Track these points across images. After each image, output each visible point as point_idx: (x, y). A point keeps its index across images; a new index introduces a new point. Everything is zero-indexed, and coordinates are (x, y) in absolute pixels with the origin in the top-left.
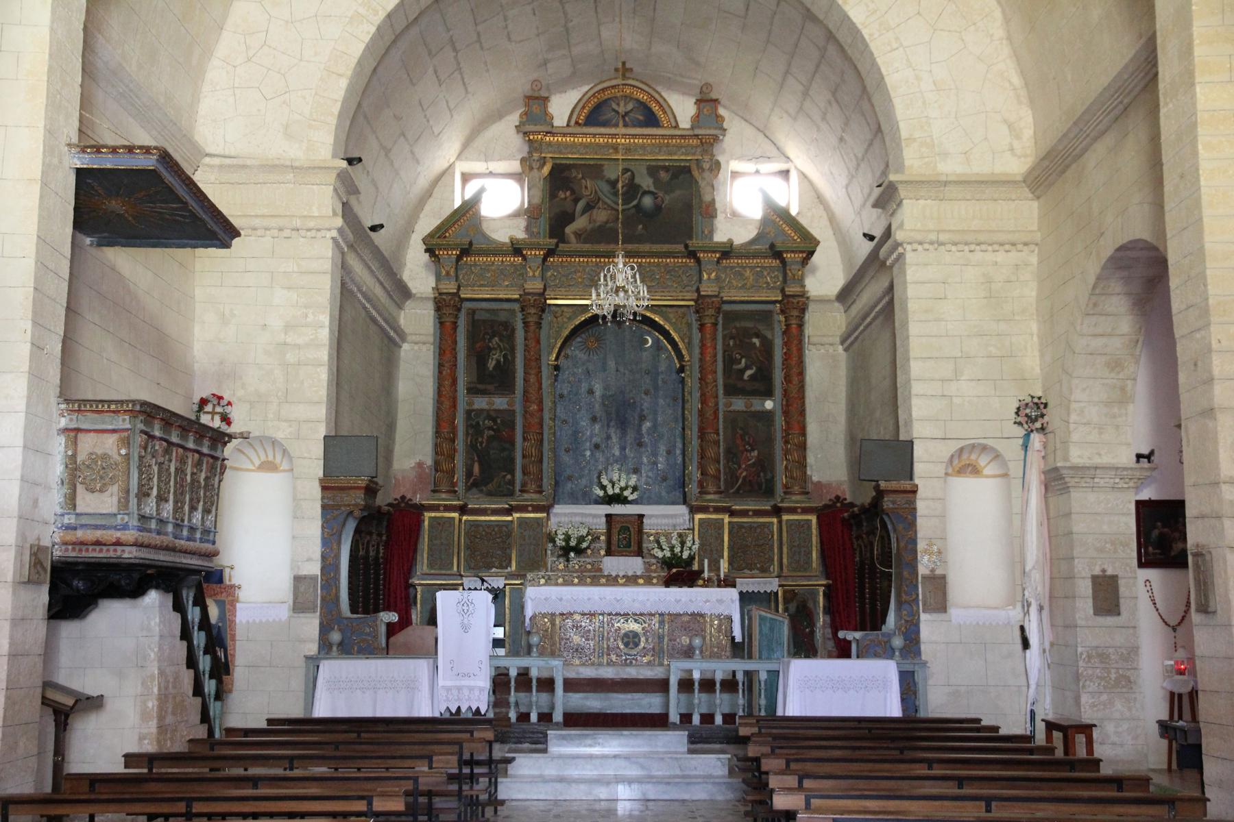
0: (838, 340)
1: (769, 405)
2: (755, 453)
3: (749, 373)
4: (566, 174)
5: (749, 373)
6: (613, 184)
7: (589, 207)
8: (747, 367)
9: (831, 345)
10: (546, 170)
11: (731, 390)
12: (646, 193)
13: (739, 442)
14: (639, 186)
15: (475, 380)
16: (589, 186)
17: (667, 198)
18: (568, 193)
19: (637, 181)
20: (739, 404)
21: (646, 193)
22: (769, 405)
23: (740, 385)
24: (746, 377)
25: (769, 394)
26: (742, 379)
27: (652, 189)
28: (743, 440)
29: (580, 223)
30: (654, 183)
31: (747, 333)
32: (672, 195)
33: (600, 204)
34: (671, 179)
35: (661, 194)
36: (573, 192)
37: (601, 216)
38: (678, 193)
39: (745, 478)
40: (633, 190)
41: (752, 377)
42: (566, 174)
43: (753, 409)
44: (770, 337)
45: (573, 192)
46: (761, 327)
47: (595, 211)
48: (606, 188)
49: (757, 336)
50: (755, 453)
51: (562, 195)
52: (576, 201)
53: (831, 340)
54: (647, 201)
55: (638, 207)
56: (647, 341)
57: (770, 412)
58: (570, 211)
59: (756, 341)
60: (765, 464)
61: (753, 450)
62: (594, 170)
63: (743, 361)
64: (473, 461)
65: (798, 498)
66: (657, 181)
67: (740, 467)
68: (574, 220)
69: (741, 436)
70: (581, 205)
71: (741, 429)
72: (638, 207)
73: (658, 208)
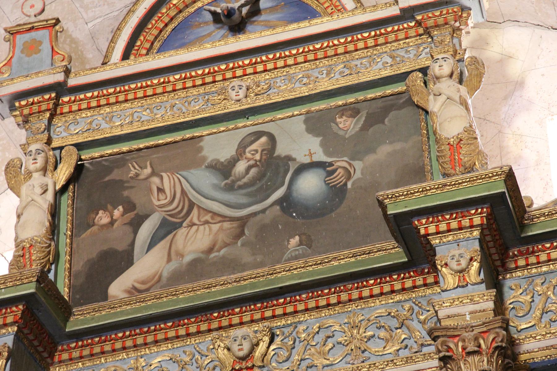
4: (115, 175)
6: (224, 169)
7: (167, 228)
10: (64, 172)
12: (303, 168)
14: (289, 158)
16: (163, 188)
17: (358, 165)
18: (118, 212)
19: (281, 150)
21: (303, 168)
27: (320, 156)
29: (148, 264)
30: (322, 144)
32: (371, 158)
33: (195, 211)
34: (365, 127)
35: (341, 163)
36: (130, 206)
37: (194, 240)
38: (384, 150)
40: (274, 167)
42: (115, 175)
45: (130, 206)
47: (182, 232)
48: (205, 179)
51: (103, 218)
52: (136, 224)
54: (310, 185)
55: (287, 203)
58: (121, 246)
62: (176, 142)
66: (331, 142)
70: (146, 230)
73: (337, 193)
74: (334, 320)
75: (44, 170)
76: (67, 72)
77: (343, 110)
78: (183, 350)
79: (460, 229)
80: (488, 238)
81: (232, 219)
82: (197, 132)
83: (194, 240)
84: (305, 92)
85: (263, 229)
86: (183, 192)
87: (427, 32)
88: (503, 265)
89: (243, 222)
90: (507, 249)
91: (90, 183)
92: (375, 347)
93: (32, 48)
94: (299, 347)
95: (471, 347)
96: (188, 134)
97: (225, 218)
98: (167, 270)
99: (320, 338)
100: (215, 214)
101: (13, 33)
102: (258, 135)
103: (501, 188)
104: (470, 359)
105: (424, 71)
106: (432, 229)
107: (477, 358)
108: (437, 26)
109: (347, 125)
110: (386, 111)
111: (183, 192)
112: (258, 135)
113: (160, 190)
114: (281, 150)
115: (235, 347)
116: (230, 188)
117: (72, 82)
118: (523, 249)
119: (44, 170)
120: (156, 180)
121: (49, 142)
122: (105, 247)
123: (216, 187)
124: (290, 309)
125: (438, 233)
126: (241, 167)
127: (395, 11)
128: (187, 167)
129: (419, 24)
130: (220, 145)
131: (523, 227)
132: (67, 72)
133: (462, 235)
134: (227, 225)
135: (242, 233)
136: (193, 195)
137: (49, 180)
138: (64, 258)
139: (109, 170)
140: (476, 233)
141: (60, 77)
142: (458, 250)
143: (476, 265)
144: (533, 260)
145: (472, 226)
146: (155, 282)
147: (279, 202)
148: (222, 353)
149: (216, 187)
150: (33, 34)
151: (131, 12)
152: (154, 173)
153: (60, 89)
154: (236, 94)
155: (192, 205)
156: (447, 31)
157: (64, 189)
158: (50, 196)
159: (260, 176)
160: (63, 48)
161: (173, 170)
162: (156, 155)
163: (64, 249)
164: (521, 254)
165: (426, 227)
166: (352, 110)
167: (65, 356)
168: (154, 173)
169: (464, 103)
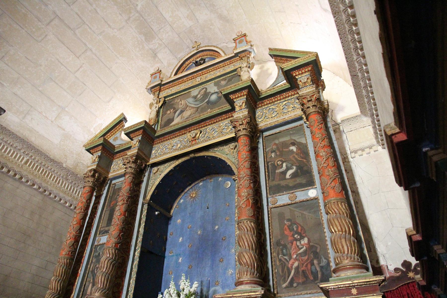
0: (374, 141)
1: (312, 193)
2: (306, 240)
3: (290, 172)
4: (172, 103)
5: (290, 172)
6: (195, 97)
7: (182, 112)
8: (288, 169)
9: (370, 148)
11: (276, 190)
13: (287, 232)
14: (210, 92)
15: (105, 225)
18: (172, 111)
19: (208, 91)
20: (283, 199)
22: (312, 193)
23: (283, 183)
24: (288, 176)
25: (311, 183)
26: (285, 179)
27: (217, 90)
28: (291, 229)
31: (285, 145)
34: (227, 83)
39: (297, 268)
40: (206, 94)
41: (294, 175)
42: (172, 103)
43: (298, 200)
44: (303, 141)
46: (297, 138)
47: (185, 112)
48: (191, 100)
49: (293, 144)
50: (306, 240)
51: (169, 112)
53: (368, 144)
56: (228, 184)
57: (316, 199)
58: (171, 118)
59: (294, 148)
60: (315, 251)
61: (302, 238)
63: (284, 165)
64: (90, 283)
65: (349, 273)
67: (290, 258)
68: (173, 121)
69: (289, 227)
71: (289, 220)
72: (208, 102)
74: (214, 126)
75: (157, 103)
76: (162, 81)
77: (222, 80)
78: (181, 138)
79: (241, 96)
80: (249, 98)
81: (196, 108)
82: (190, 90)
83: (187, 114)
84: (214, 77)
85: (202, 109)
86: (186, 104)
87: (242, 59)
88: (256, 106)
89: (198, 108)
90: (256, 103)
91: (166, 105)
92: (224, 131)
93: (155, 78)
94: (207, 134)
95: (241, 123)
96: (188, 91)
97: (194, 108)
98: (181, 121)
99: (212, 131)
100: (192, 107)
101: (152, 75)
102: (203, 89)
103: (250, 84)
104: (240, 126)
105: (240, 67)
106: (234, 97)
107: (242, 126)
108: (243, 57)
109: (223, 83)
110: (232, 78)
111: (186, 104)
112: (203, 89)
113: (181, 104)
114: (208, 91)
115: (192, 135)
116: (196, 101)
117: (163, 83)
118: (260, 102)
119: (157, 103)
120: (181, 102)
121: (158, 97)
122: (168, 118)
123: (193, 101)
124: (205, 125)
125: (235, 98)
126: (199, 96)
127: (233, 55)
128: (187, 98)
129: (239, 57)
130: (194, 92)
131: (259, 96)
132: (162, 81)
133: (242, 98)
134: (194, 109)
135: (198, 110)
136: (188, 104)
137: (157, 105)
138: (160, 122)
139: (171, 102)
140: (245, 97)
141: (160, 82)
142: (240, 102)
143: (244, 104)
144: (263, 104)
145: (244, 95)
146: (178, 124)
147: (207, 102)
148: (189, 137)
149: (193, 101)
150: (156, 75)
151: (176, 66)
152: (180, 101)
153: (160, 85)
154: (198, 80)
155: (187, 106)
156: (246, 58)
157: (161, 107)
158: (157, 109)
159: (203, 97)
160: (161, 76)
161: (184, 99)
162: (181, 97)
163: (160, 120)
164: (260, 103)
165: (232, 97)
166: (225, 79)
167: (156, 142)
168: (180, 101)
169: (249, 72)
